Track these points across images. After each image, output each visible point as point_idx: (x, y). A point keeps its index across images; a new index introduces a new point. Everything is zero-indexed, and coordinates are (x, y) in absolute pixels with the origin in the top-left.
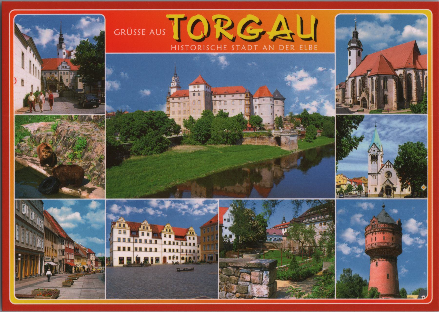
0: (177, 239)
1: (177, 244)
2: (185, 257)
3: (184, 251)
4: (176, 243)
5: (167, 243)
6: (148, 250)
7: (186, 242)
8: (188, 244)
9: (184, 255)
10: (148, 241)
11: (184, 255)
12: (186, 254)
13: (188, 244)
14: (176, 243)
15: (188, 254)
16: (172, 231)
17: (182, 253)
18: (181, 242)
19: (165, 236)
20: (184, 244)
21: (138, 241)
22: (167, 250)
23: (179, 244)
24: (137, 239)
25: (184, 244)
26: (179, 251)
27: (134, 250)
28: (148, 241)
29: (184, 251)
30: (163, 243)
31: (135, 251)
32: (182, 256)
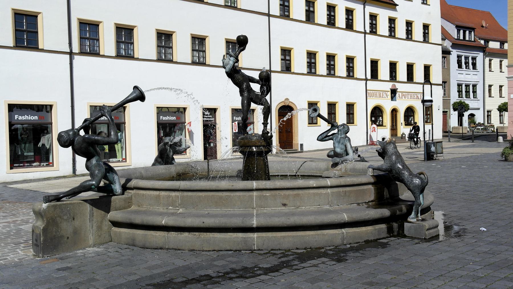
2: (387, 106)
3: (384, 72)
7: (392, 14)
8: (401, 30)
11: (379, 93)
12: (394, 92)
13: (401, 30)
15: (400, 87)
17: (372, 85)
18: (371, 9)
20: (383, 27)
23: (358, 25)
25: (383, 27)
27: (76, 49)
29: (384, 72)
31: (82, 53)
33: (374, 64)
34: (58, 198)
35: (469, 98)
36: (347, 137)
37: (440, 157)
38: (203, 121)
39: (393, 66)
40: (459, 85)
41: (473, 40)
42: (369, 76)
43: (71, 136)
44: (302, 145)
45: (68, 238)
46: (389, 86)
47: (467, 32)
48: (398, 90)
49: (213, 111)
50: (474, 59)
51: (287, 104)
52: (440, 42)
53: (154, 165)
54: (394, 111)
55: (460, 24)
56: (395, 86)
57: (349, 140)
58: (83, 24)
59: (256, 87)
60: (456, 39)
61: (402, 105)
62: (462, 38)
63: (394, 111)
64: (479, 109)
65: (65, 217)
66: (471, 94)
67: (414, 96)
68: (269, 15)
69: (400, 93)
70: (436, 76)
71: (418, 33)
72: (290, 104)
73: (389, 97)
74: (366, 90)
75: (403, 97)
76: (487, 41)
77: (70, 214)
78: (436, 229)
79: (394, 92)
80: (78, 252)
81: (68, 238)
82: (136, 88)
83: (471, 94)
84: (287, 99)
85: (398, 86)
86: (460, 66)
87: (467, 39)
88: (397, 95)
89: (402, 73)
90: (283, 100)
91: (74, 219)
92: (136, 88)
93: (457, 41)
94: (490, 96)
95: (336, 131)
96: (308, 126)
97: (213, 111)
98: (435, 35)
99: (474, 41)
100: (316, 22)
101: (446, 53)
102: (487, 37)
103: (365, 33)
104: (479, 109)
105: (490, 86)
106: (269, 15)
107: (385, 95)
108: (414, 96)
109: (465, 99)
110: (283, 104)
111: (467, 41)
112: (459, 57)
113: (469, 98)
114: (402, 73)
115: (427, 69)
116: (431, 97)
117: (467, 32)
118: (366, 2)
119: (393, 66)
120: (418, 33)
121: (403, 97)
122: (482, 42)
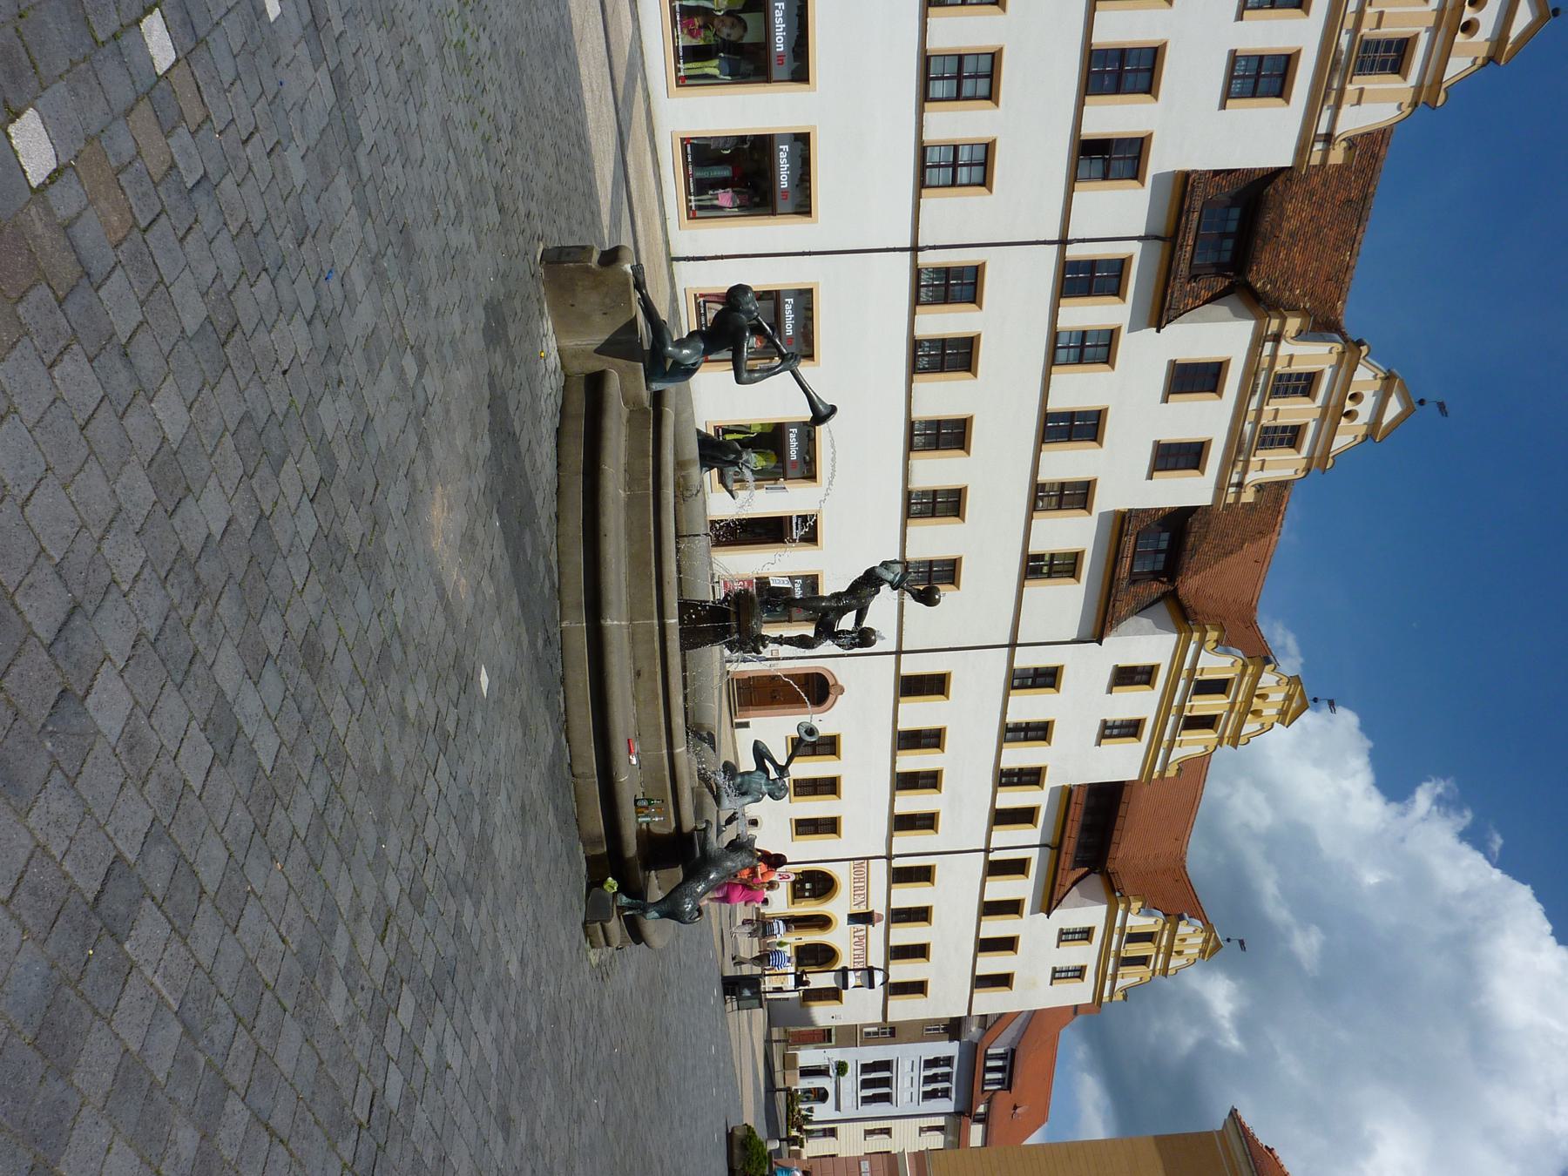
0: (1077, 813)
1: (1002, 817)
2: (838, 907)
3: (908, 896)
4: (1013, 798)
5: (1029, 706)
6: (936, 471)
8: (996, 927)
9: (862, 886)
10: (1065, 462)
11: (862, 886)
12: (865, 918)
13: (996, 927)
14: (1013, 798)
15: (876, 932)
16: (1193, 744)
17: (879, 871)
19: (1127, 676)
20: (1002, 888)
21: (1085, 314)
22: (919, 713)
24: (1117, 291)
25: (1002, 888)
26: (907, 842)
28: (1065, 462)
29: (908, 896)
30: (1027, 659)
31: (917, 272)
32: (840, 872)
33: (923, 875)
34: (640, 286)
35: (862, 1088)
36: (763, 796)
37: (732, 1004)
38: (791, 517)
39: (920, 915)
40: (886, 1065)
41: (986, 1088)
42: (897, 863)
43: (745, 307)
44: (746, 725)
45: (572, 305)
46: (878, 906)
47: (999, 1076)
48: (870, 926)
49: (811, 537)
50: (946, 1093)
51: (832, 691)
52: (976, 1012)
53: (699, 432)
54: (823, 922)
55: (1019, 1054)
56: (879, 921)
57: (758, 800)
58: (977, 271)
59: (847, 622)
60: (986, 1051)
61: (840, 937)
62: (990, 1064)
63: (823, 922)
64: (838, 1108)
65: (607, 301)
66: (869, 1092)
67: (859, 963)
68: (1013, 645)
69: (864, 932)
70: (904, 1009)
71: (992, 964)
72: (831, 697)
73: (856, 910)
74: (868, 859)
75: (857, 939)
76: (983, 1119)
77: (613, 307)
78: (603, 943)
79: (865, 918)
80: (550, 323)
81: (572, 305)
82: (833, 409)
83: (869, 1092)
84: (842, 691)
85: (880, 926)
86: (930, 1064)
87: (988, 1076)
88: (863, 927)
89: (905, 934)
90: (840, 683)
91: (605, 314)
92: (833, 409)
93: (983, 1055)
94: (869, 1133)
95: (773, 775)
96: (787, 737)
97: (811, 537)
98: (991, 1002)
99: (983, 1091)
100: (1004, 745)
101: (953, 1028)
102: (995, 1119)
103: (987, 851)
104: (838, 1108)
105: (887, 1131)
106: (1013, 645)
107: (860, 899)
108: (859, 963)
109: (860, 1078)
110: (831, 682)
111: (984, 1076)
112: (948, 1061)
113: (862, 1088)
114: (905, 934)
115: (919, 988)
116: (855, 987)
117: (999, 1076)
118: (1052, 848)
119: (920, 915)
120: (992, 964)
121: (857, 939)
122: (981, 1109)
